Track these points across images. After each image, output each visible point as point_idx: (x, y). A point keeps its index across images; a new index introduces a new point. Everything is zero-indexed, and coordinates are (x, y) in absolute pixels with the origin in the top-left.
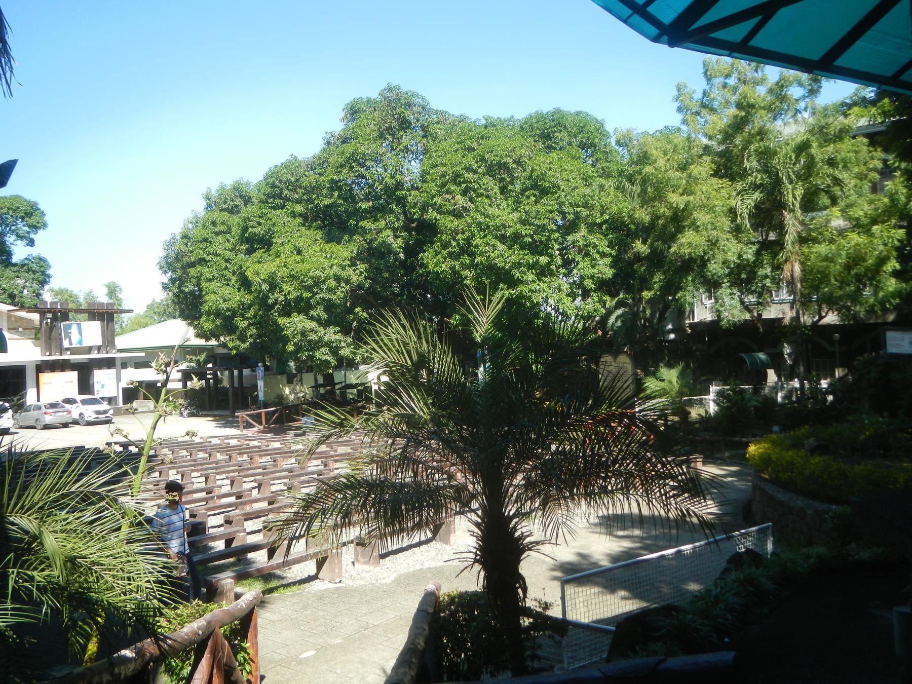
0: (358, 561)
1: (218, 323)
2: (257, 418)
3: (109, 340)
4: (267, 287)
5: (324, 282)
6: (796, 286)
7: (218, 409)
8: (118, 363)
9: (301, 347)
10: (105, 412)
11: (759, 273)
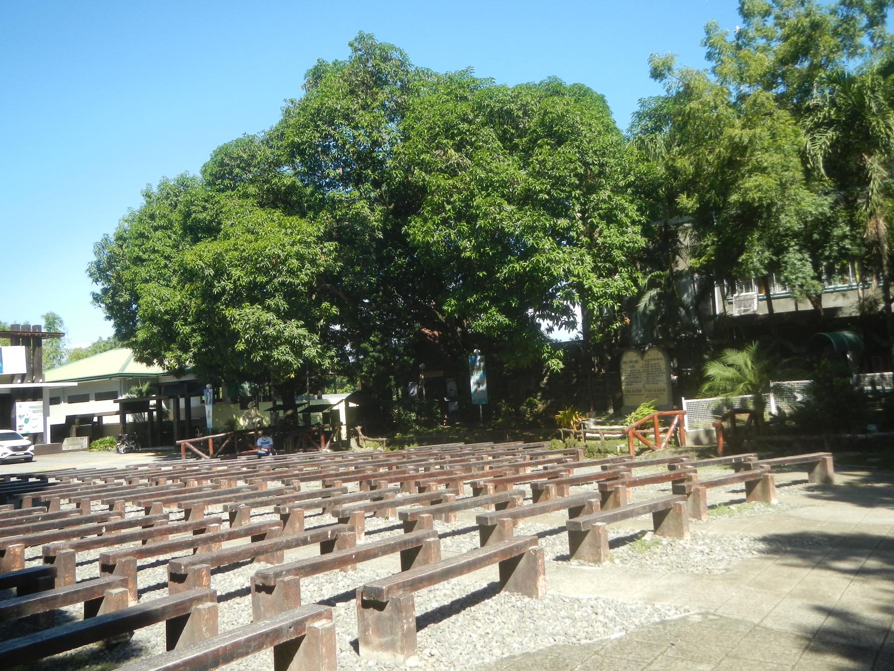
0: (367, 643)
1: (155, 331)
2: (204, 447)
3: (35, 368)
4: (212, 272)
5: (284, 262)
6: (882, 248)
7: (161, 445)
8: (47, 396)
9: (255, 345)
10: (24, 448)
11: (835, 234)
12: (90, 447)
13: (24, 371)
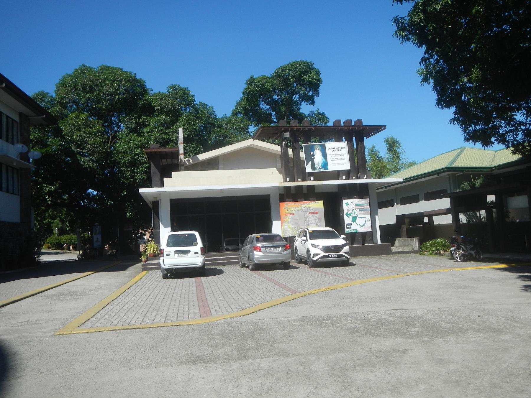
10: (338, 248)
12: (420, 251)
13: (347, 166)
